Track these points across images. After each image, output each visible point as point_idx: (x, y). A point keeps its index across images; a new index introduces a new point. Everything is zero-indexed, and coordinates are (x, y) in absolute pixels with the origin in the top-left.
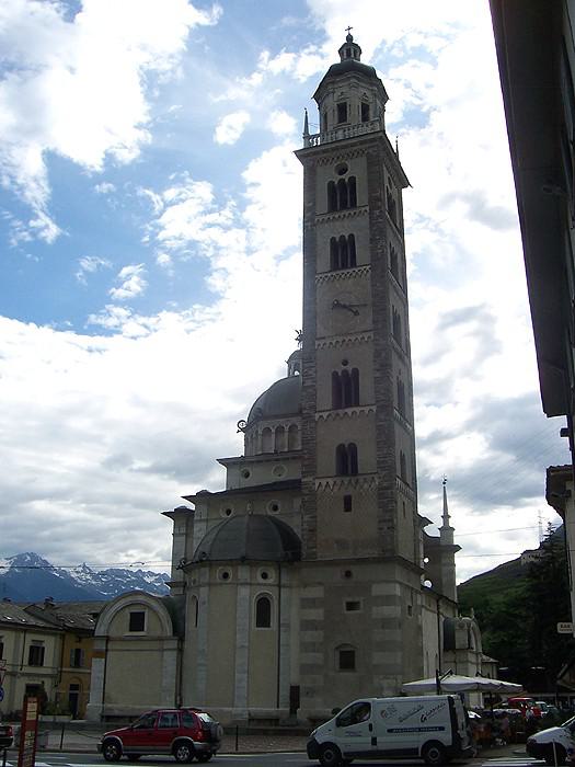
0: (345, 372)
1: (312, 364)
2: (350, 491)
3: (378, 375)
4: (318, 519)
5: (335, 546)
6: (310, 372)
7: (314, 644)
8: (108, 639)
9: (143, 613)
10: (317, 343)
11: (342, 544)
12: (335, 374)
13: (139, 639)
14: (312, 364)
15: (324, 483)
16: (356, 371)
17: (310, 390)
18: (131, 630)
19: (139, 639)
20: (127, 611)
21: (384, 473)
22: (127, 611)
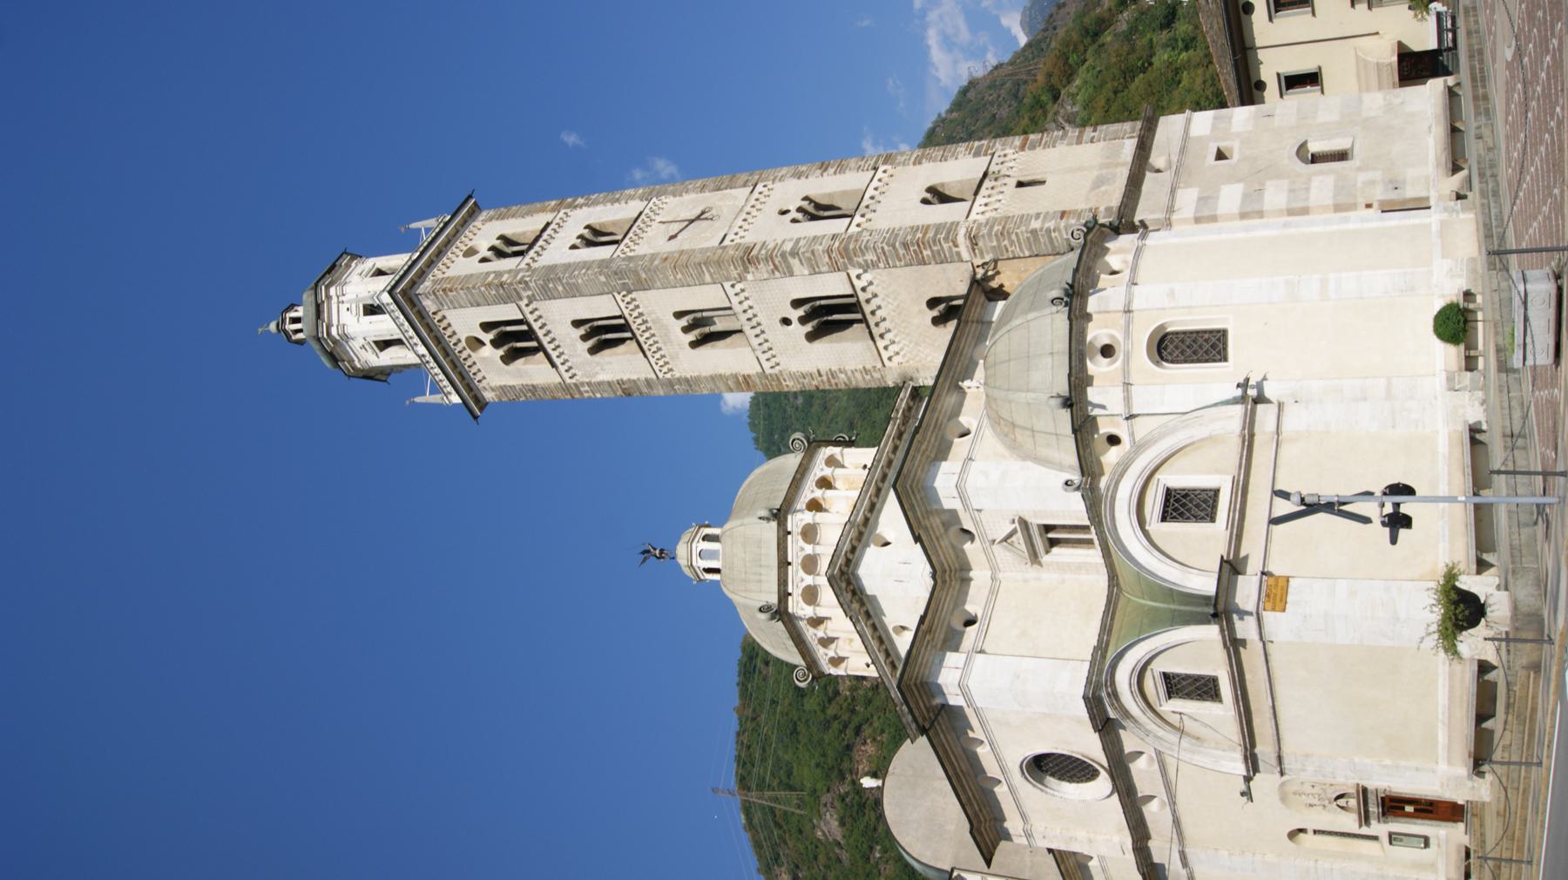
0: (800, 210)
1: (757, 247)
2: (1013, 182)
3: (831, 171)
4: (1044, 211)
5: (1103, 188)
6: (771, 246)
7: (1291, 191)
8: (1232, 567)
9: (1169, 493)
10: (727, 242)
11: (1099, 183)
12: (794, 221)
13: (1242, 489)
14: (757, 247)
15: (983, 208)
16: (806, 198)
17: (802, 243)
18: (1213, 520)
19: (1242, 489)
20: (1155, 526)
21: (998, 145)
22: (1155, 526)
